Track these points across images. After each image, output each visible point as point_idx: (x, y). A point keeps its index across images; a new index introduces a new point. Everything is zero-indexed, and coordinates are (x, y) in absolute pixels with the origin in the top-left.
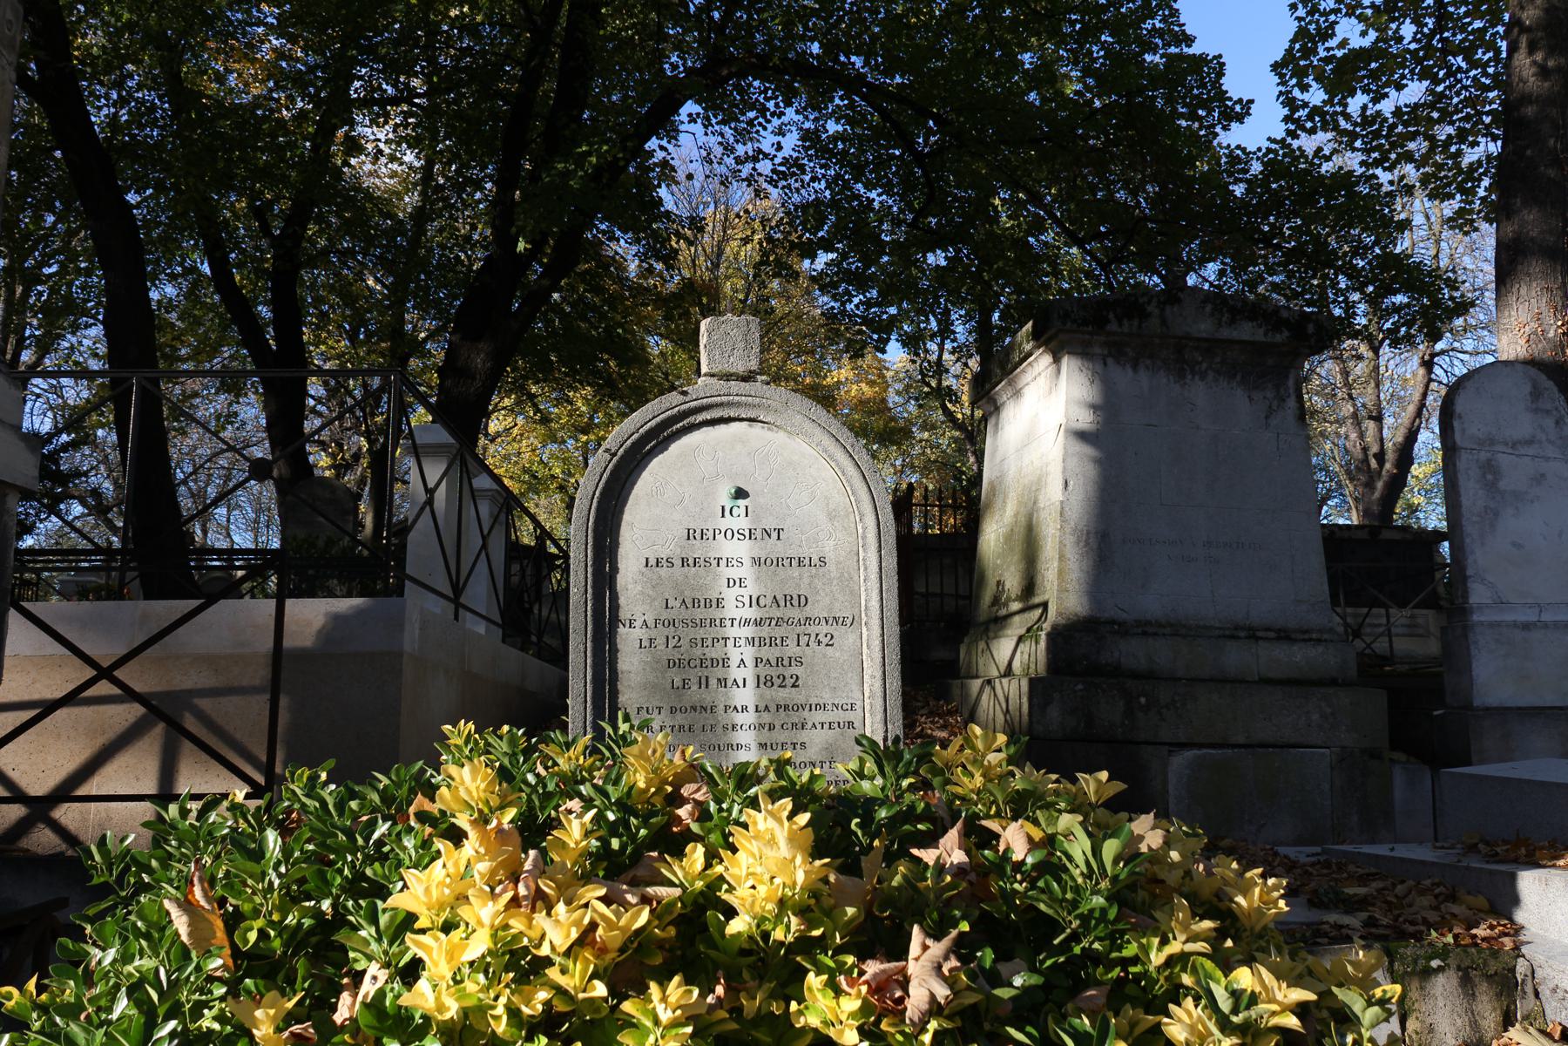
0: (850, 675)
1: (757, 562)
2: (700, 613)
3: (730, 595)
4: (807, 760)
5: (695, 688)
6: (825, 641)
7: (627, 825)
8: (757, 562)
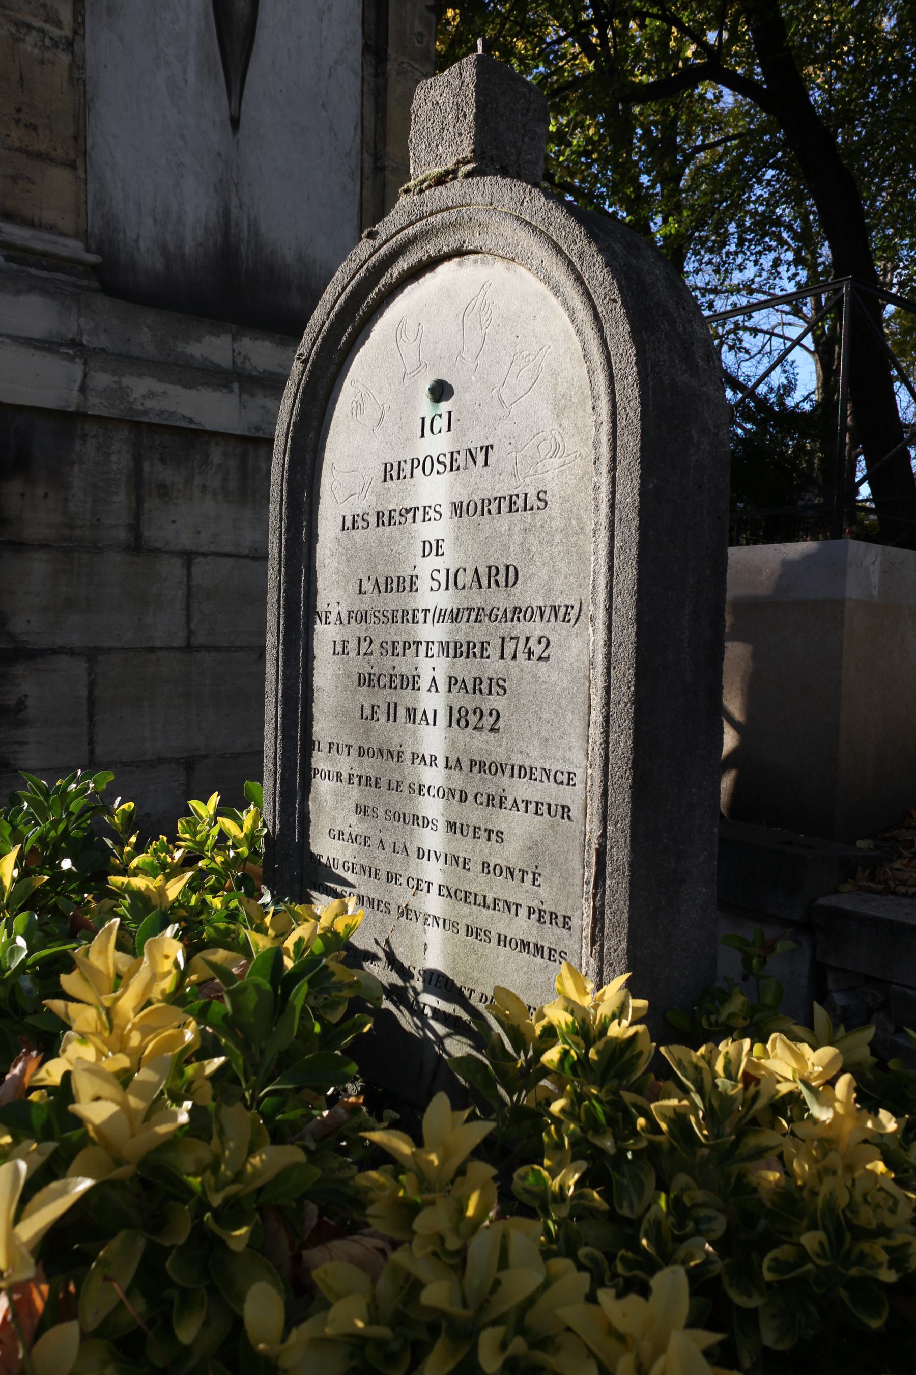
0: (569, 717)
1: (458, 509)
2: (393, 601)
3: (426, 566)
4: (504, 864)
5: (383, 719)
6: (538, 649)
8: (458, 509)
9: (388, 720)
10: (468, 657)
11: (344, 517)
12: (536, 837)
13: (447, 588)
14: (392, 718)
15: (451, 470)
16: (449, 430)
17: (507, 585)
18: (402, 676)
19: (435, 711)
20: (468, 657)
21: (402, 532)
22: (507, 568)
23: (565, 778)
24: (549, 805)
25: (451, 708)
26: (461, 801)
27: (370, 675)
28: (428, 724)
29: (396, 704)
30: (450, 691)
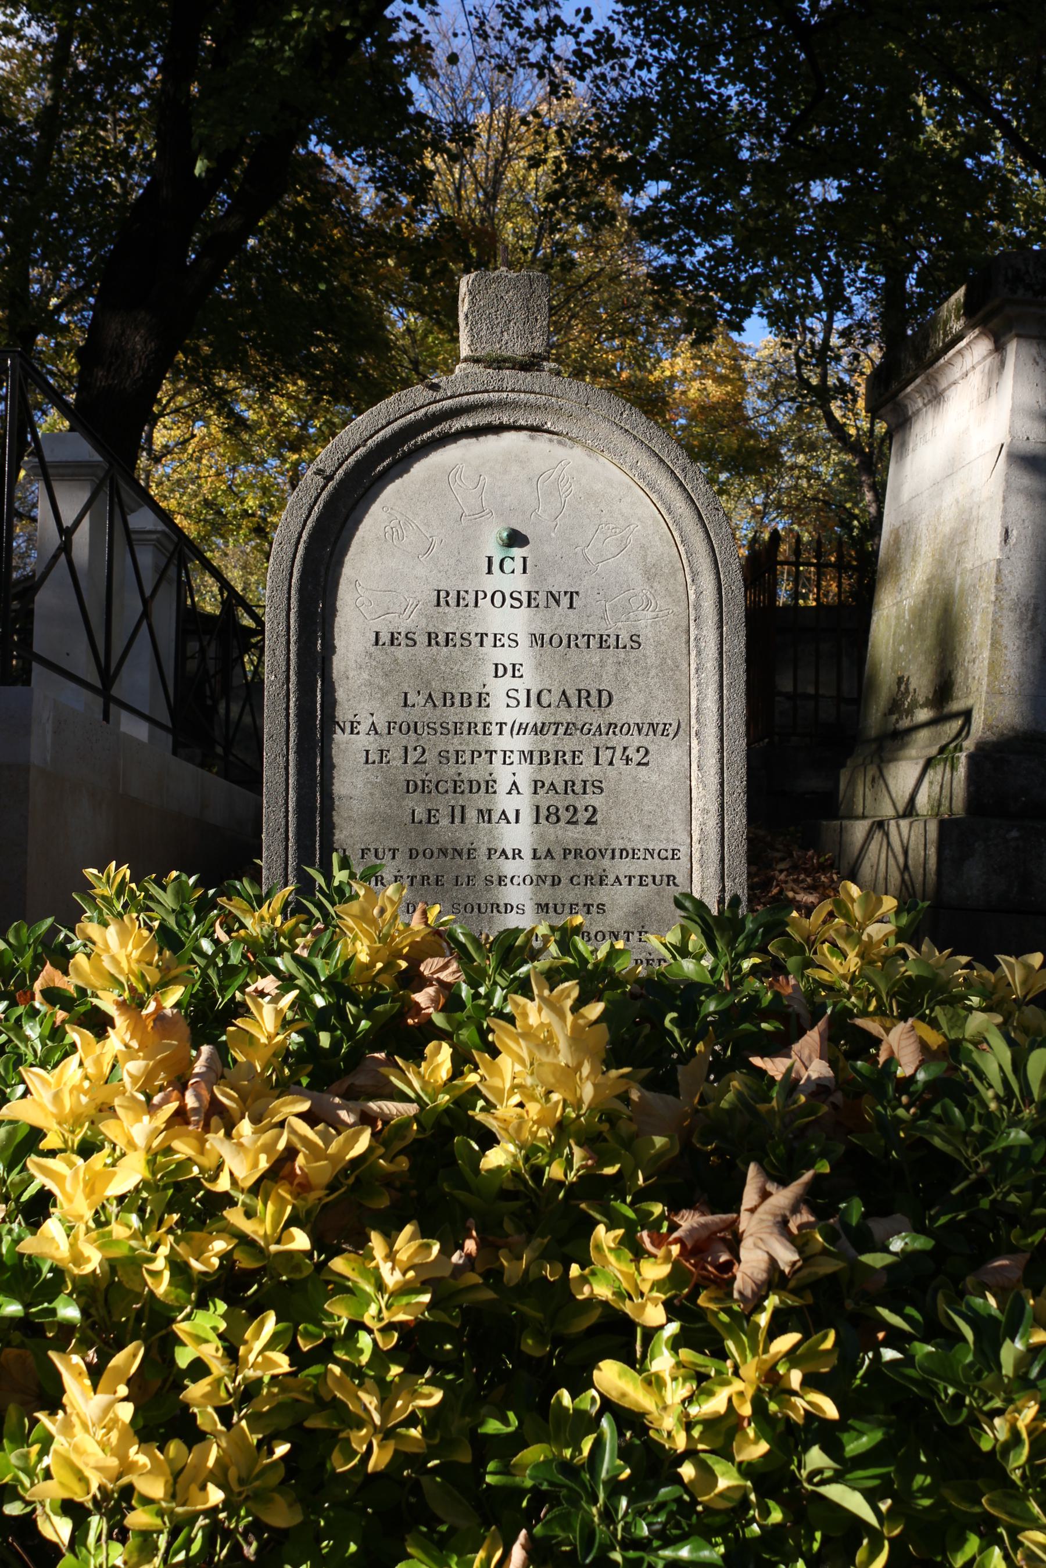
0: (671, 808)
1: (538, 640)
2: (453, 715)
3: (498, 688)
4: (607, 929)
5: (445, 822)
6: (636, 757)
7: (342, 1015)
9: (453, 822)
10: (556, 763)
11: (377, 634)
12: (641, 903)
13: (528, 705)
14: (457, 820)
15: (529, 605)
16: (524, 572)
17: (600, 706)
18: (471, 782)
19: (517, 811)
20: (556, 763)
21: (465, 654)
22: (600, 692)
23: (670, 854)
24: (654, 877)
25: (538, 807)
26: (553, 885)
27: (423, 781)
28: (508, 822)
29: (463, 807)
30: (535, 792)
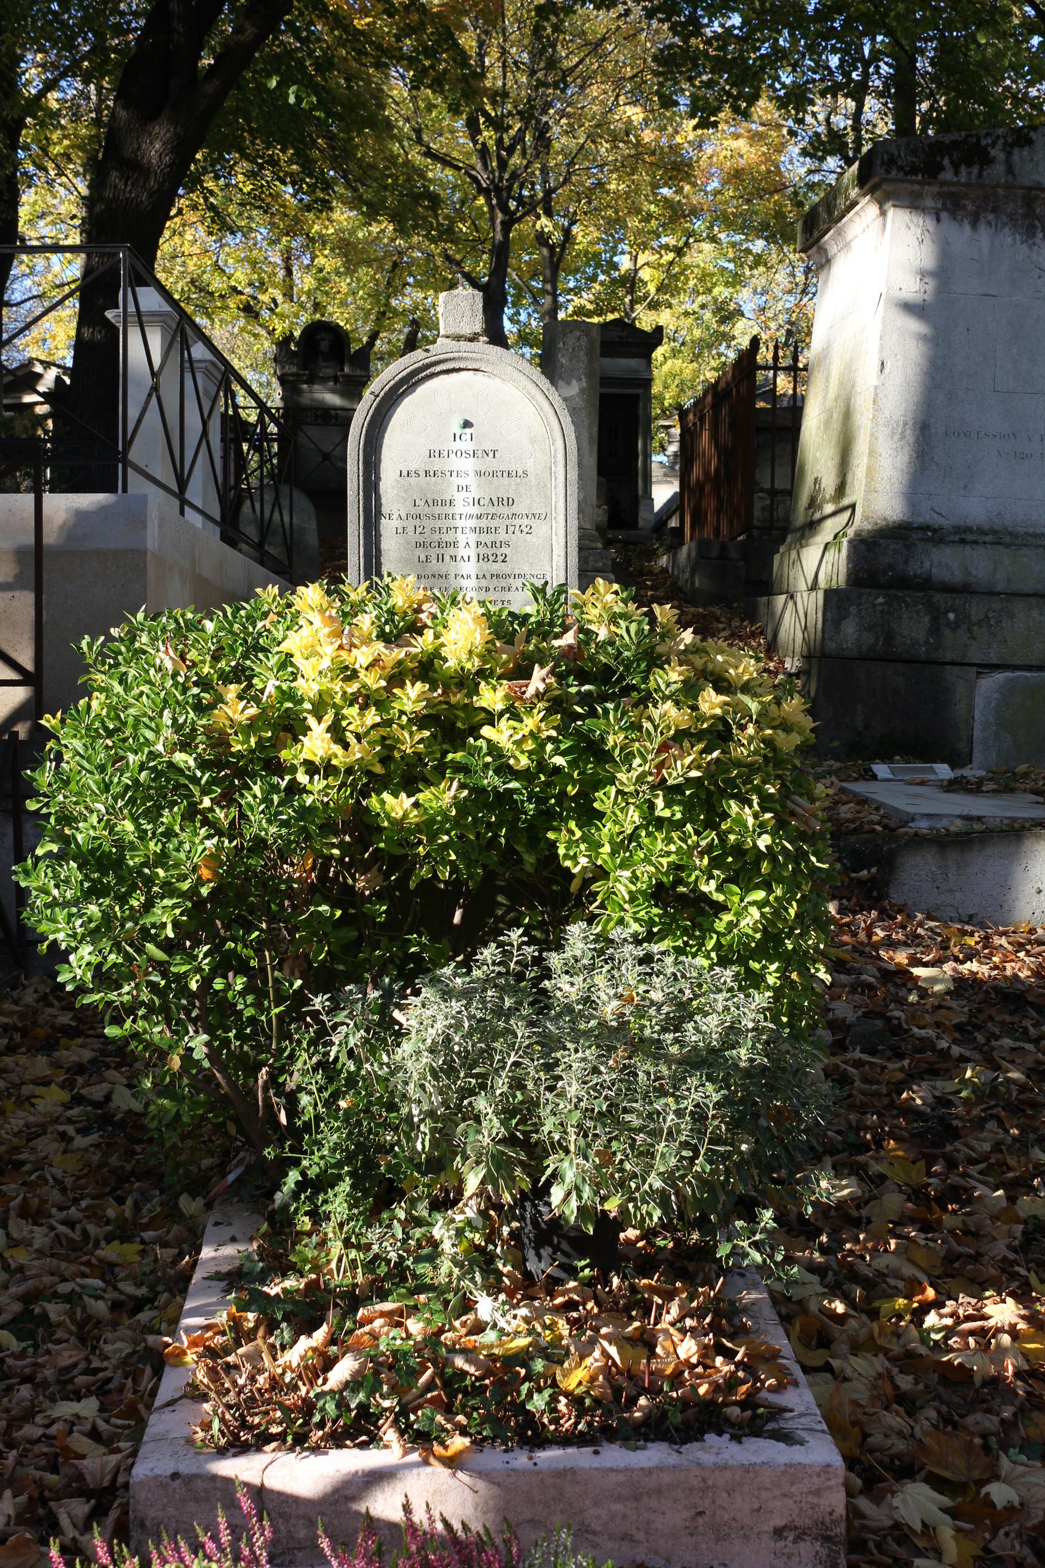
1: (479, 474)
2: (438, 510)
3: (459, 497)
5: (434, 561)
6: (526, 530)
7: (393, 621)
8: (479, 474)
